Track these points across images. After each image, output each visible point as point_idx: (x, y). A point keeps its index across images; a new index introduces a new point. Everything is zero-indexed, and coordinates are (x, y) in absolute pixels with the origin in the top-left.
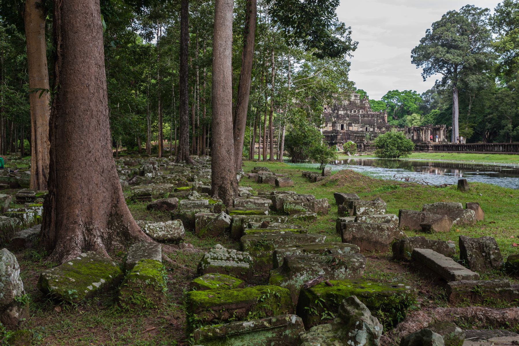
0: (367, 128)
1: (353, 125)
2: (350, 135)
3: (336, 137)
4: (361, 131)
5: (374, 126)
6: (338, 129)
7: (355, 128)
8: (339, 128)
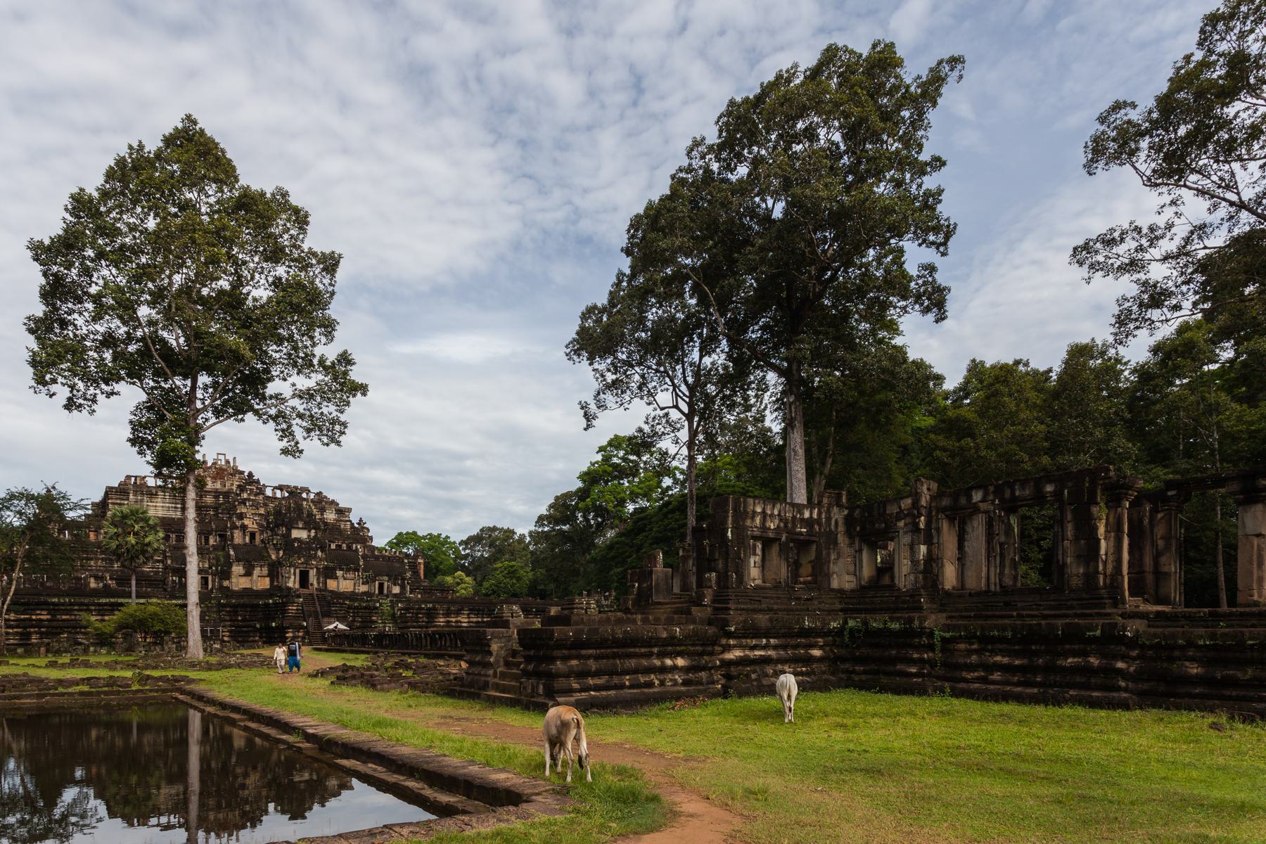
0: (381, 586)
1: (339, 573)
2: (329, 604)
3: (281, 608)
4: (364, 593)
5: (403, 579)
6: (290, 584)
7: (344, 584)
8: (293, 582)
